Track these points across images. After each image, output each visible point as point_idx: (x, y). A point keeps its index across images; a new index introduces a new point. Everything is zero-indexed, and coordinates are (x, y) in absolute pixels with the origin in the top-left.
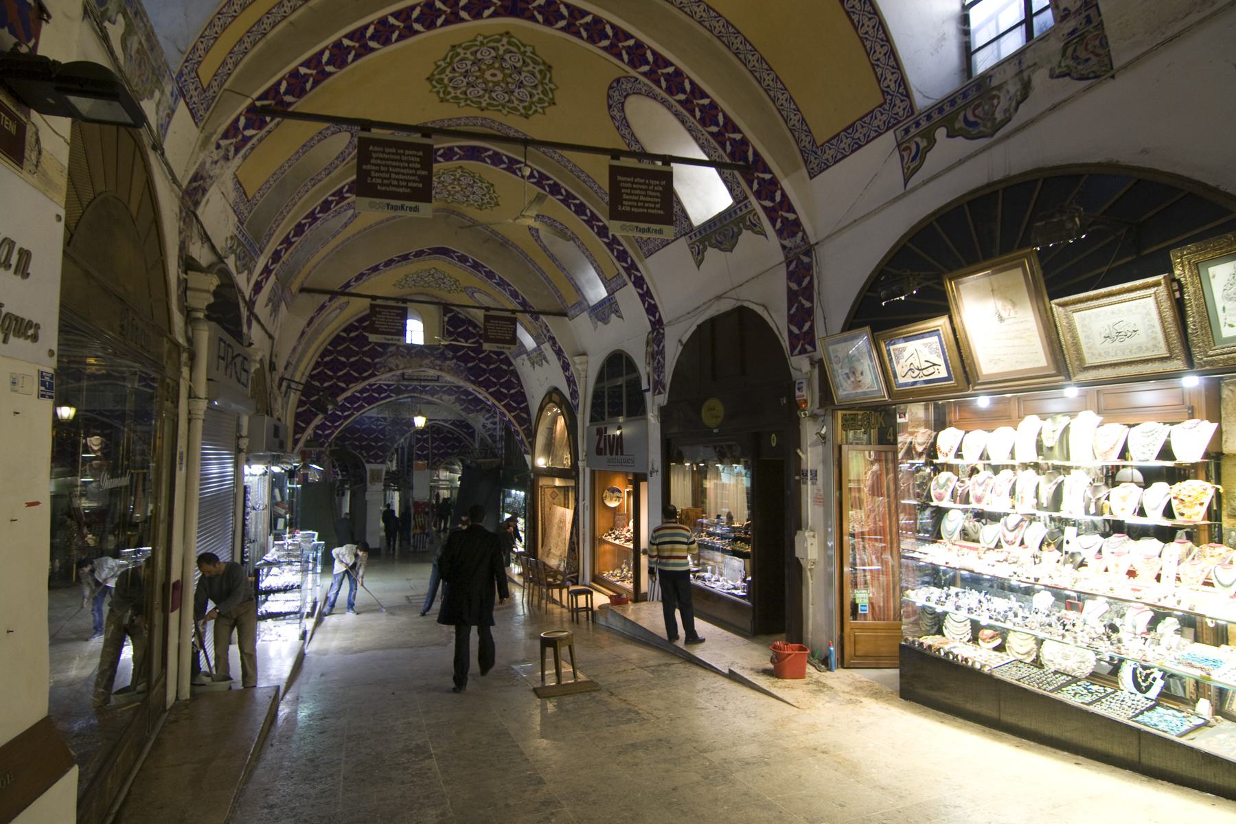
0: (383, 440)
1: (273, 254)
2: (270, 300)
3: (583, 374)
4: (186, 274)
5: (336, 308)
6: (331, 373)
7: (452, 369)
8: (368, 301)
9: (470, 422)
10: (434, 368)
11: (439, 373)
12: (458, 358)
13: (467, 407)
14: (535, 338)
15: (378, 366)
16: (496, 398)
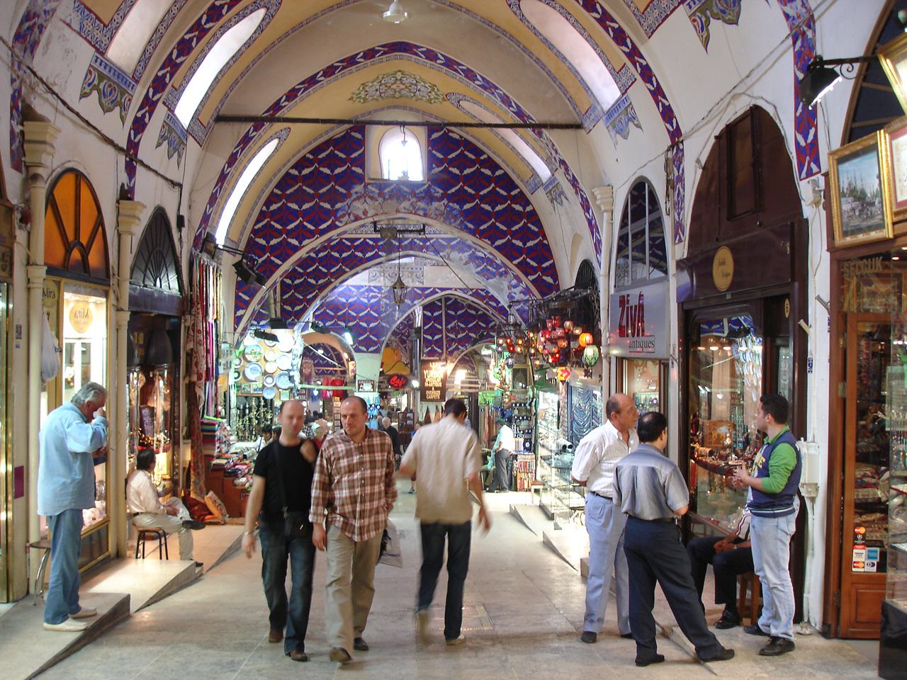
0: (375, 319)
1: (154, 82)
2: (163, 138)
4: (22, 124)
5: (271, 139)
6: (279, 227)
7: (442, 214)
9: (493, 292)
10: (415, 214)
11: (425, 220)
12: (451, 198)
13: (485, 269)
14: (548, 162)
15: (340, 213)
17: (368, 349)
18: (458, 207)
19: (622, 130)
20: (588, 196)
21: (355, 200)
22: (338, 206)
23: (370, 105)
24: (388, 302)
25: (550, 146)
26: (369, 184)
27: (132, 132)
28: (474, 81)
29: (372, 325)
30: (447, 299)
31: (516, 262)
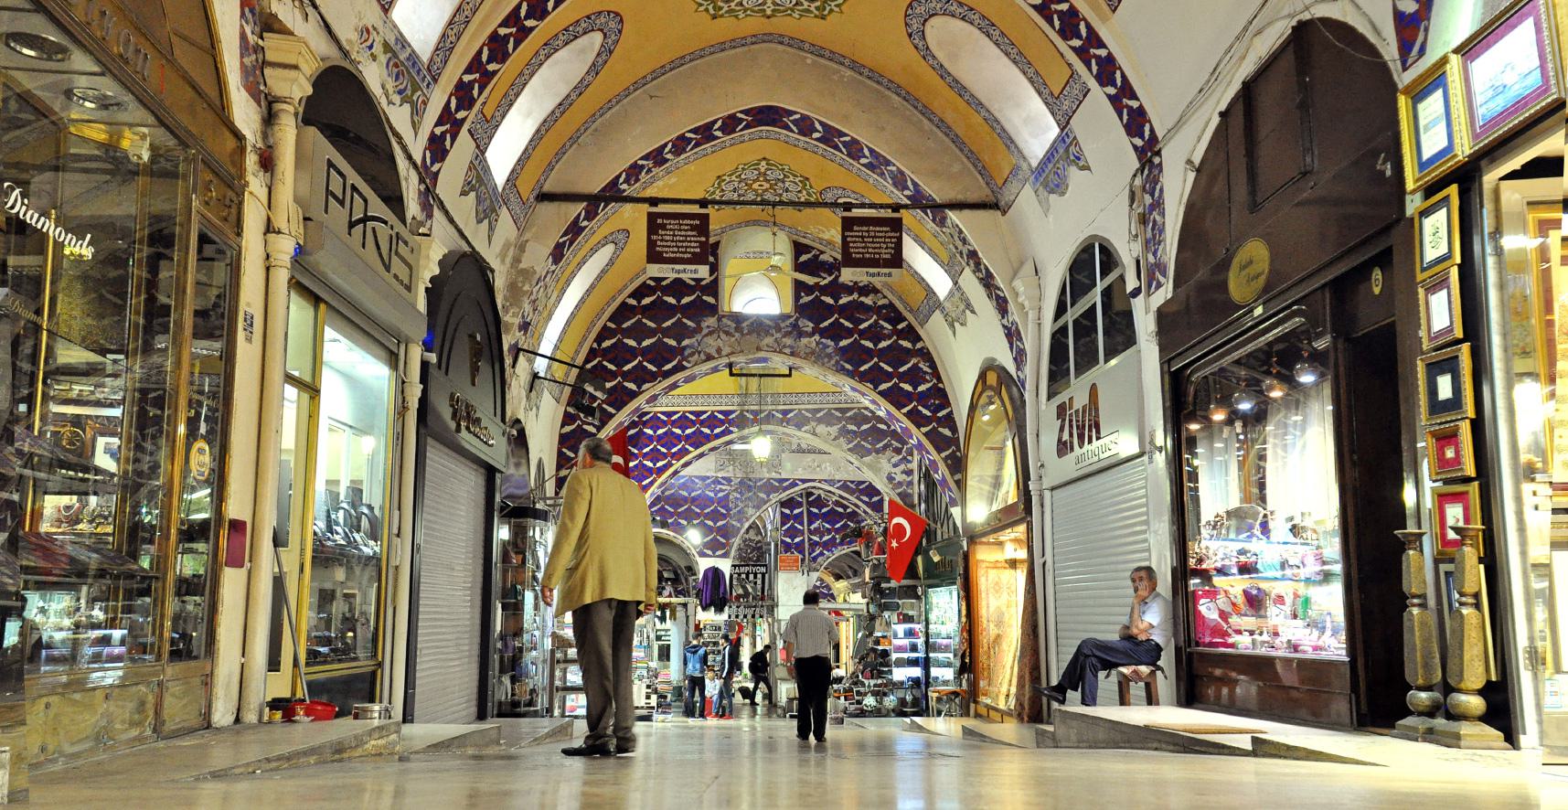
0: (724, 516)
3: (1031, 315)
6: (613, 368)
7: (813, 353)
10: (780, 352)
12: (824, 333)
18: (832, 344)
19: (1057, 186)
22: (685, 343)
24: (739, 496)
26: (723, 316)
31: (905, 410)
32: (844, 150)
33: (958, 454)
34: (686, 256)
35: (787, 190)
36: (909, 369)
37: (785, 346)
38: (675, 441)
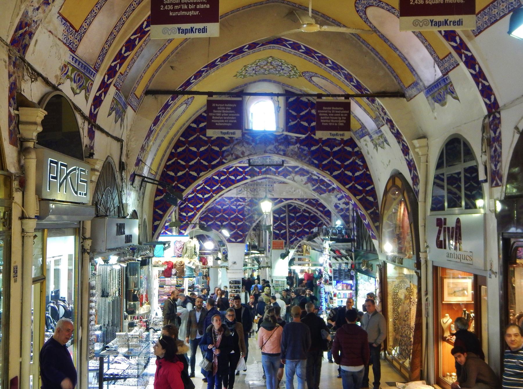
0: (242, 220)
1: (108, 70)
2: (112, 109)
3: (423, 159)
4: (18, 110)
5: (182, 104)
6: (184, 163)
7: (296, 154)
8: (205, 98)
10: (278, 154)
11: (284, 158)
15: (225, 154)
16: (340, 182)
17: (236, 240)
20: (408, 144)
21: (236, 144)
22: (224, 149)
23: (248, 79)
24: (249, 208)
25: (380, 110)
26: (246, 133)
27: (93, 107)
28: (325, 64)
29: (239, 224)
30: (289, 206)
31: (348, 186)
32: (317, 59)
33: (377, 211)
34: (228, 124)
35: (283, 70)
36: (350, 163)
37: (280, 150)
38: (215, 183)
